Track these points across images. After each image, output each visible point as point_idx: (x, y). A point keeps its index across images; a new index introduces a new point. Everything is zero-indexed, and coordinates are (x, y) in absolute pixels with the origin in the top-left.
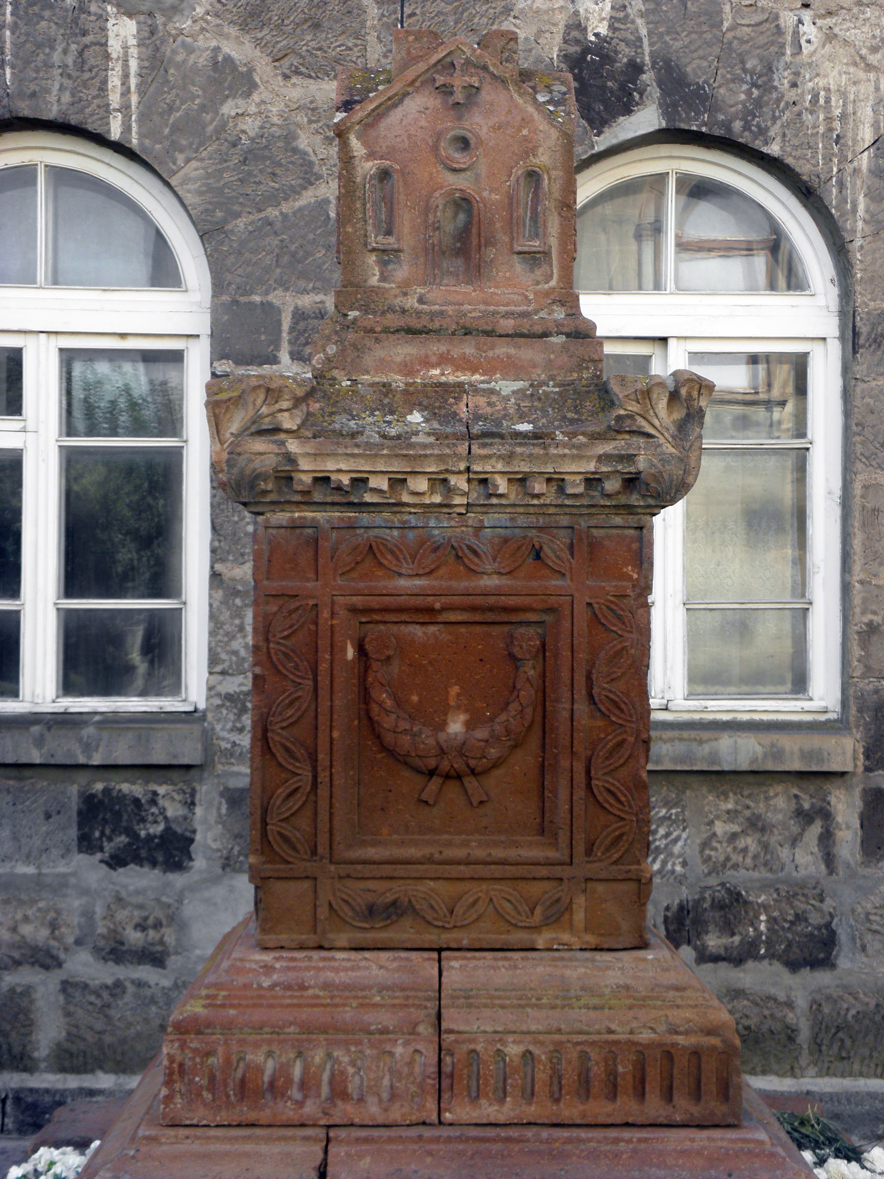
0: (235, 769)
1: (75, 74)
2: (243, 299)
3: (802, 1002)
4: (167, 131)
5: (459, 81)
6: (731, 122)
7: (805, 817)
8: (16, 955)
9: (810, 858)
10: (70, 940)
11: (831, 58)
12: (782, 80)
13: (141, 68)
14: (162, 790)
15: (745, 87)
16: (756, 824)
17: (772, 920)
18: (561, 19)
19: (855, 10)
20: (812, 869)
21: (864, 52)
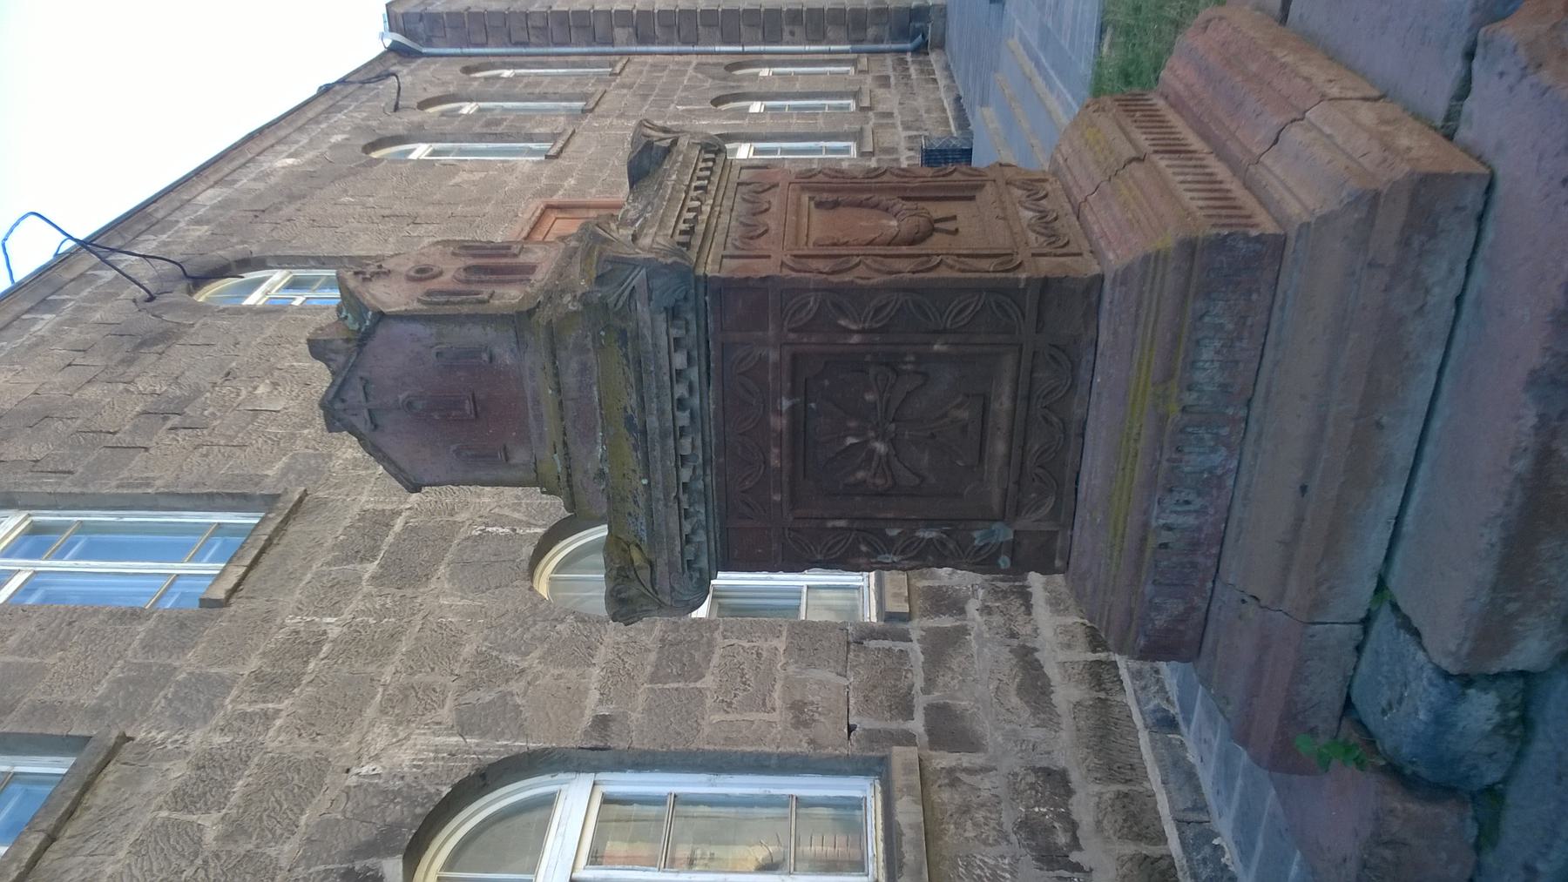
6: (415, 815)
9: (986, 780)
11: (391, 757)
17: (1038, 804)
21: (394, 740)
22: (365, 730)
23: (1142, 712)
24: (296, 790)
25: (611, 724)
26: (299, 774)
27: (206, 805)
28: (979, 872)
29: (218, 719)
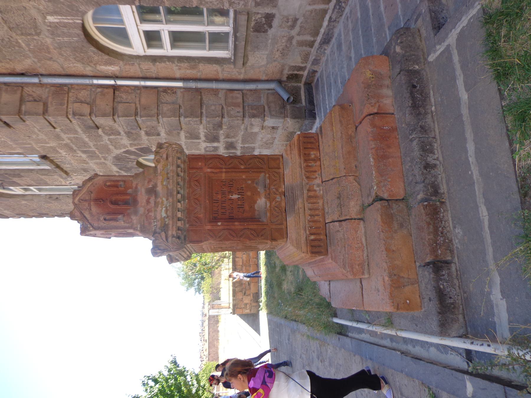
0: (249, 5)
14: (254, 18)
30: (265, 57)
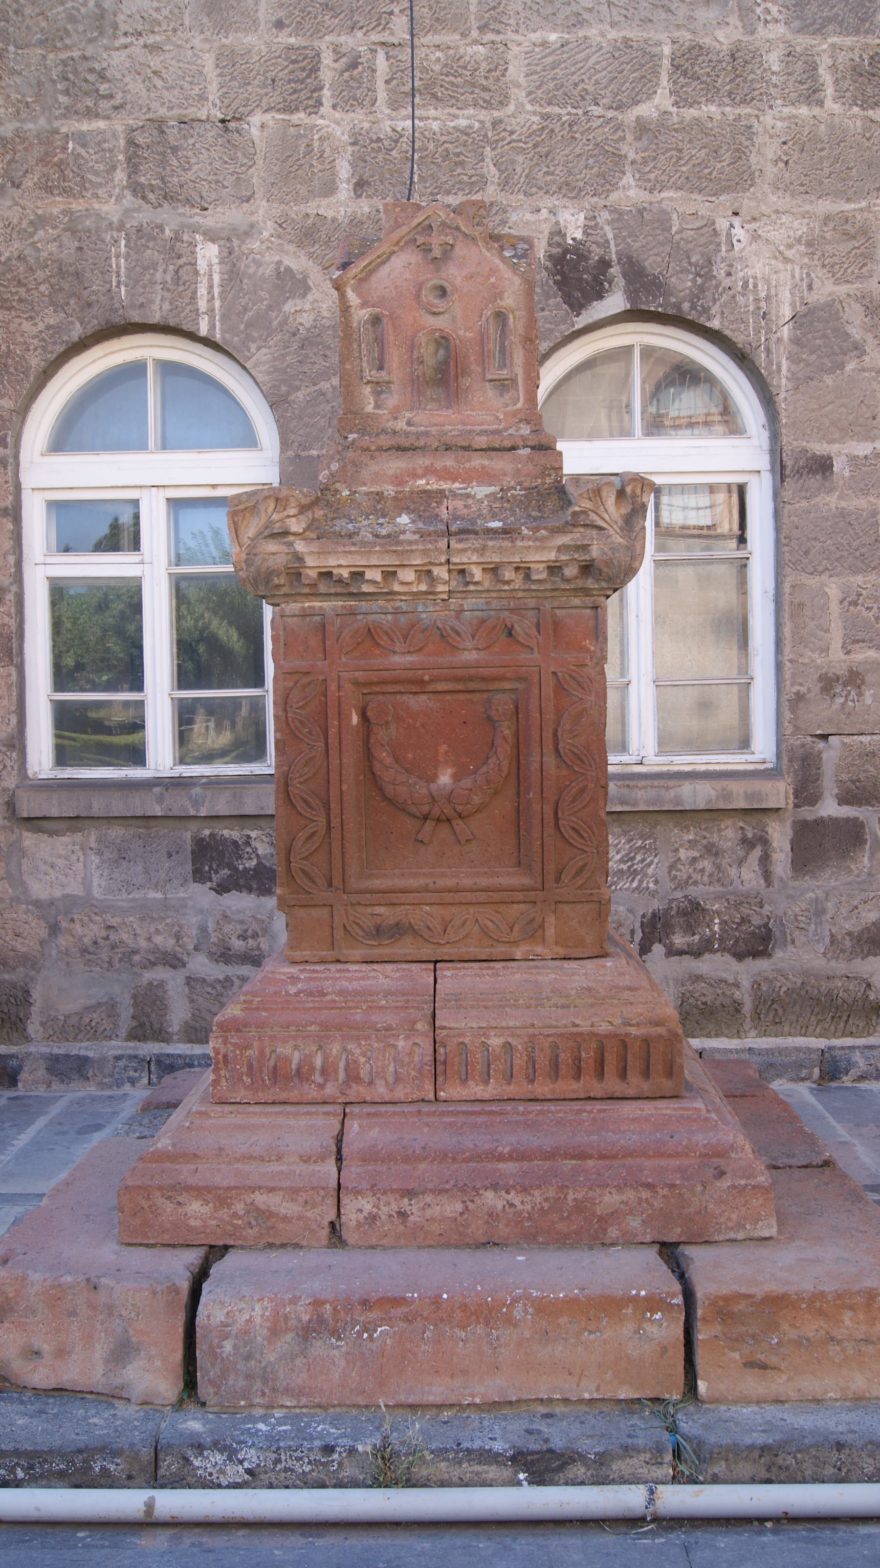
1: (172, 287)
2: (303, 454)
3: (746, 983)
4: (242, 327)
5: (436, 240)
6: (680, 303)
7: (748, 844)
8: (152, 958)
9: (752, 875)
10: (191, 947)
11: (757, 253)
12: (719, 271)
13: (222, 280)
14: (253, 834)
15: (691, 276)
16: (712, 851)
17: (723, 923)
18: (546, 228)
19: (774, 217)
20: (754, 883)
21: (781, 248)
22: (795, 210)
23: (852, 1048)
24: (707, 171)
25: (819, 477)
26: (728, 165)
27: (682, 87)
28: (639, 858)
29: (803, 41)
30: (75, 888)
